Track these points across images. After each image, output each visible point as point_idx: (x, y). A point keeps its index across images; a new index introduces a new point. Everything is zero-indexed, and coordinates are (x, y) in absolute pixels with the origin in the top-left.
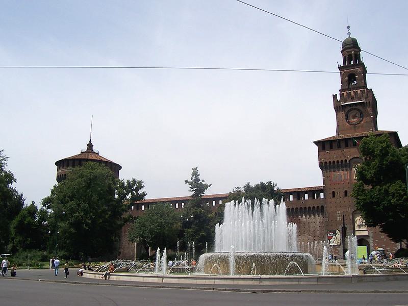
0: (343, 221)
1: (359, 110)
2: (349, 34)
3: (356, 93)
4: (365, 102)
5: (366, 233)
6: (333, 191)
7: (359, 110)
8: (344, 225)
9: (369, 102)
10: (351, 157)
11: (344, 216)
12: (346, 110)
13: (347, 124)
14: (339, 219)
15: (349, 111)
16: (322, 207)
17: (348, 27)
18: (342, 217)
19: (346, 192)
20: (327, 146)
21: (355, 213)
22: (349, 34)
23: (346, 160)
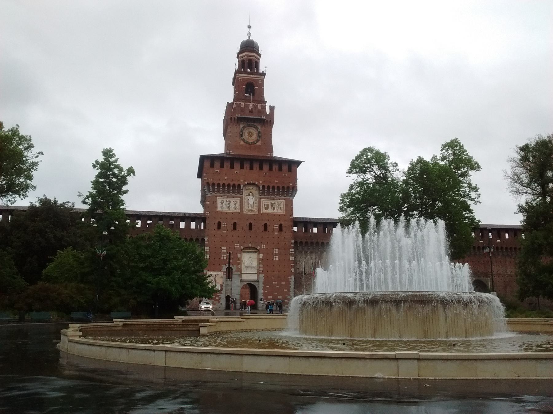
0: (228, 260)
1: (257, 128)
2: (249, 34)
3: (256, 107)
4: (266, 120)
5: (254, 277)
6: (220, 220)
7: (257, 128)
8: (229, 266)
9: (270, 121)
10: (246, 183)
11: (230, 253)
12: (242, 125)
13: (241, 142)
14: (224, 257)
15: (244, 127)
16: (203, 240)
17: (249, 27)
18: (228, 255)
19: (235, 224)
20: (217, 164)
21: (244, 252)
22: (249, 34)
23: (239, 186)
